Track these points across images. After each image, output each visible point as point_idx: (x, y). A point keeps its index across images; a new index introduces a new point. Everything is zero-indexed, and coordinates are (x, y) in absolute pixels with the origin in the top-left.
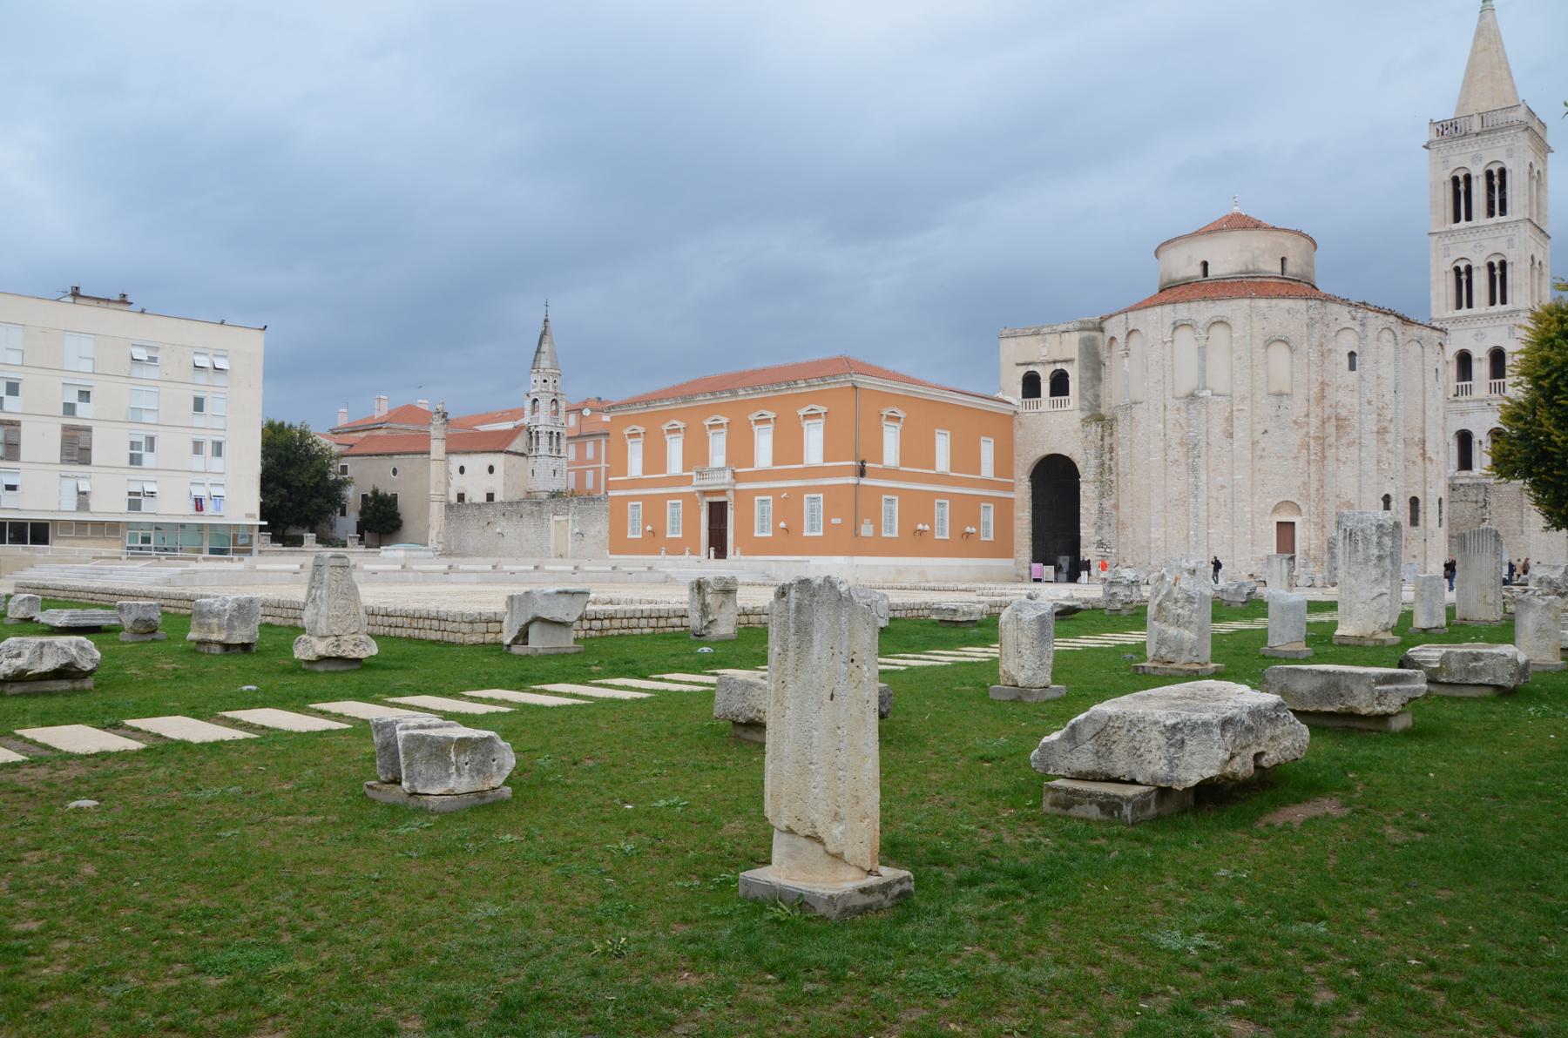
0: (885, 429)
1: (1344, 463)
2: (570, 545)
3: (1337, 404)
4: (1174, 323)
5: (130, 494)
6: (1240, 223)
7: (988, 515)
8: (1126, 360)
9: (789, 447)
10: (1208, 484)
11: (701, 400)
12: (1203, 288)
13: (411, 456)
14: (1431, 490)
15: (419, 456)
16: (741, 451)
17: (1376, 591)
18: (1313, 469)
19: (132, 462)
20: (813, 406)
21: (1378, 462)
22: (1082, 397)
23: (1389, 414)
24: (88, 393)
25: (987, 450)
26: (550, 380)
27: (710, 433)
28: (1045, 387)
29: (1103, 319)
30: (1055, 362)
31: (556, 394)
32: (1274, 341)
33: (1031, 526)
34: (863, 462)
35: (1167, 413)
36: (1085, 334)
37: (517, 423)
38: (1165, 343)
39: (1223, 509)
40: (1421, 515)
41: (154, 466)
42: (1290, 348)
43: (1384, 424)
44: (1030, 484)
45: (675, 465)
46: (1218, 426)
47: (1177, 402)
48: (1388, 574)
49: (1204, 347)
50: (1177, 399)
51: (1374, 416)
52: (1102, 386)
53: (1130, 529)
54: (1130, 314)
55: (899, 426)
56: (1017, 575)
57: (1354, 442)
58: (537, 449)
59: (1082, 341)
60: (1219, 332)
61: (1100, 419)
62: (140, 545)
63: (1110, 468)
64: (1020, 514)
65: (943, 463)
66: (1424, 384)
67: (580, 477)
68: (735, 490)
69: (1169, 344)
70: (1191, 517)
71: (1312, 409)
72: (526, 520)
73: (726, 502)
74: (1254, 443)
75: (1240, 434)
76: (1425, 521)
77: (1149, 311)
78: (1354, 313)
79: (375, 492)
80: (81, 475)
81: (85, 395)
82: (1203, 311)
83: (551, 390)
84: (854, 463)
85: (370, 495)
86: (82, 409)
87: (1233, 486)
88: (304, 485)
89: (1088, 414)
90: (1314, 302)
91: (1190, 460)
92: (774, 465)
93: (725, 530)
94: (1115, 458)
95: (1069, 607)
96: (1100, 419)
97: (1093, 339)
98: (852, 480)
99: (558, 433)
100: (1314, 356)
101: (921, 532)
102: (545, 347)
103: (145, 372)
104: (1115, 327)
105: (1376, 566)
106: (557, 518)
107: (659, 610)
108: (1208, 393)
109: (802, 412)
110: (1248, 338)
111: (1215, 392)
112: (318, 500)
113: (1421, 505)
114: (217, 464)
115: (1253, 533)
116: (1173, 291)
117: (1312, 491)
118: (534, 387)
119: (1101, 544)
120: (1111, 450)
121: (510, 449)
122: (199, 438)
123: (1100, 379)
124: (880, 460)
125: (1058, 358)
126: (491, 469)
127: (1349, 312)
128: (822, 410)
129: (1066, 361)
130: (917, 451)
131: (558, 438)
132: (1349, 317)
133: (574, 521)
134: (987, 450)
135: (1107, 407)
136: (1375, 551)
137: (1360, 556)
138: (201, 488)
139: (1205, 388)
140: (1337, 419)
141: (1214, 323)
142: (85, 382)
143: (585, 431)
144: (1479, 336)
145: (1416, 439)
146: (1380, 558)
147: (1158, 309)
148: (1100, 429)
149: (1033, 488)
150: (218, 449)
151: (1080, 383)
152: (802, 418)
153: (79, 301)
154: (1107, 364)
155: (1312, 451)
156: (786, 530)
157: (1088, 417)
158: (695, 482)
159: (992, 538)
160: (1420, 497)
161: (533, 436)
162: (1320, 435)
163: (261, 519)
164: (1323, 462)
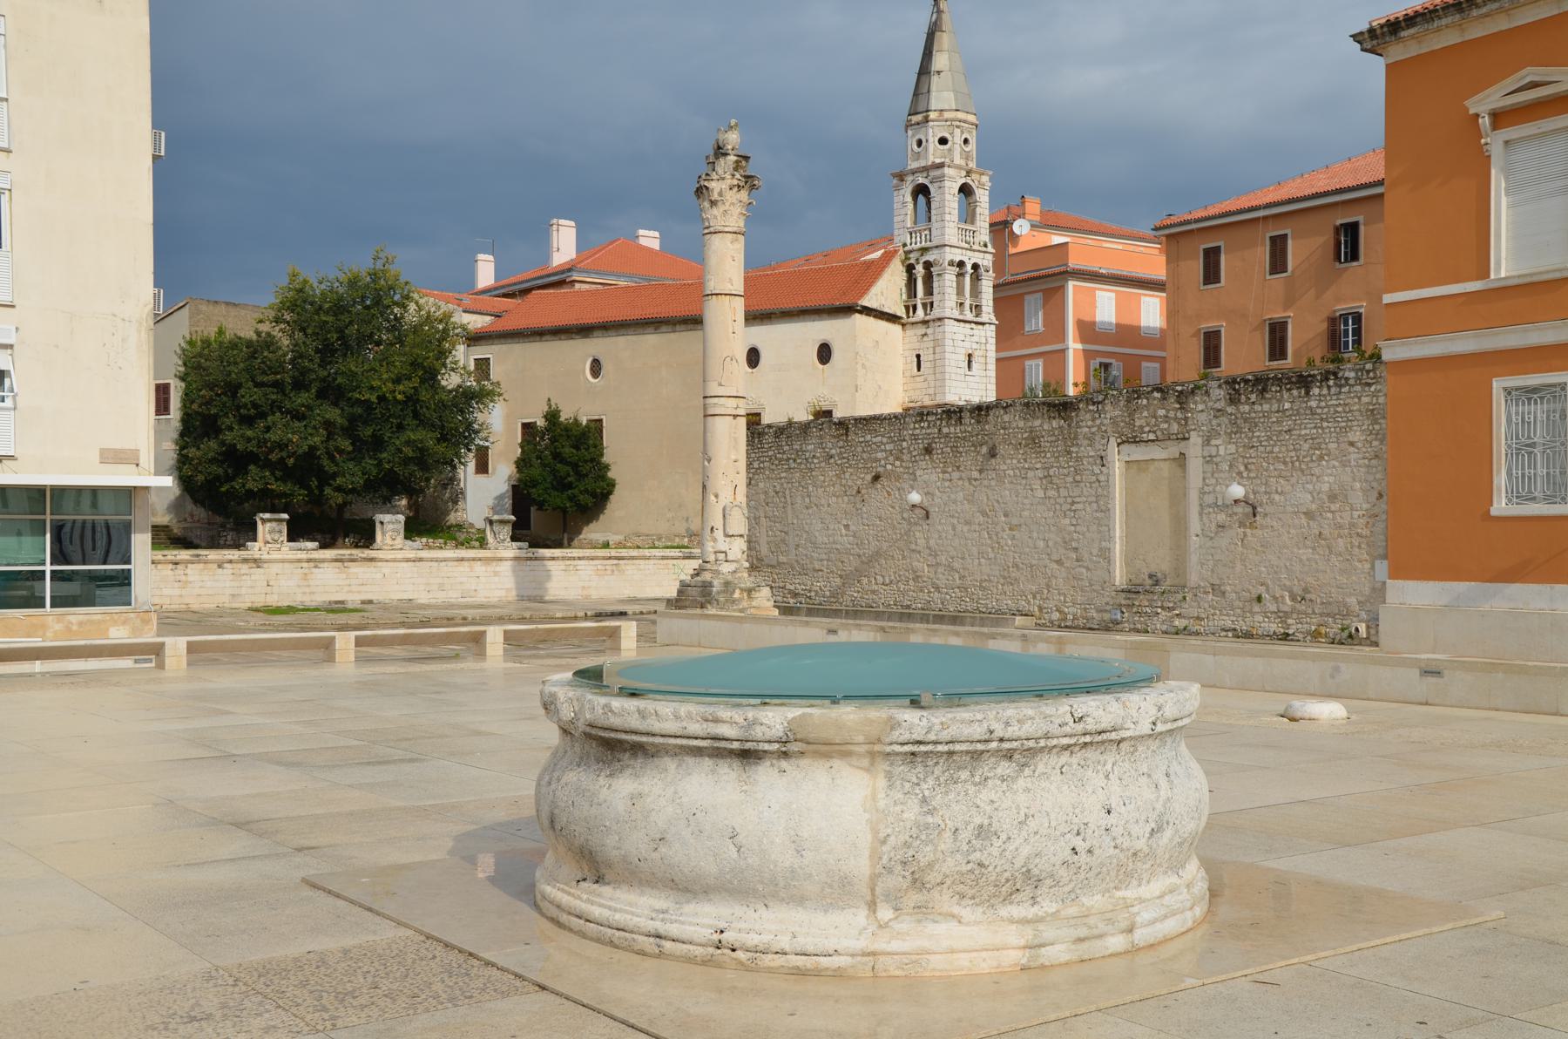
31: (969, 173)
72: (1009, 462)
79: (552, 416)
83: (958, 161)
85: (541, 423)
88: (382, 398)
99: (975, 267)
102: (940, 61)
106: (1138, 453)
118: (917, 156)
121: (866, 302)
133: (1209, 460)
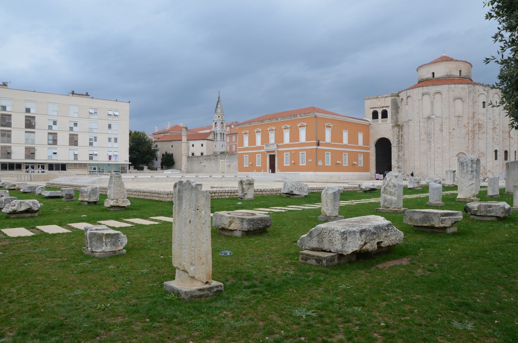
0: (326, 130)
1: (481, 139)
2: (226, 169)
3: (479, 119)
4: (423, 93)
5: (90, 155)
6: (446, 59)
7: (361, 158)
8: (407, 106)
9: (294, 137)
10: (434, 147)
11: (267, 122)
12: (432, 81)
13: (177, 141)
15: (179, 141)
16: (279, 138)
17: (471, 183)
18: (470, 141)
19: (90, 145)
20: (302, 123)
21: (493, 139)
22: (392, 118)
23: (497, 123)
24: (77, 123)
25: (360, 137)
26: (221, 116)
27: (270, 132)
28: (380, 116)
29: (399, 93)
30: (383, 107)
31: (222, 121)
32: (456, 99)
33: (375, 161)
34: (319, 141)
35: (421, 123)
36: (393, 98)
37: (211, 130)
38: (419, 100)
39: (440, 155)
40: (508, 157)
41: (96, 146)
42: (462, 101)
43: (495, 126)
44: (375, 147)
45: (259, 143)
46: (437, 127)
47: (423, 120)
48: (475, 177)
49: (433, 101)
50: (424, 119)
51: (492, 123)
52: (399, 115)
53: (408, 162)
54: (408, 91)
55: (331, 129)
56: (371, 178)
57: (484, 132)
58: (217, 139)
59: (392, 100)
60: (438, 96)
61: (398, 126)
62: (93, 170)
63: (402, 142)
64: (372, 158)
65: (345, 141)
67: (231, 147)
68: (278, 151)
69: (421, 100)
70: (429, 158)
71: (470, 121)
72: (212, 161)
73: (275, 155)
74: (450, 133)
75: (445, 130)
76: (510, 159)
77: (414, 89)
78: (484, 88)
79: (166, 153)
80: (75, 149)
81: (76, 124)
82: (432, 89)
84: (316, 141)
85: (165, 154)
86: (75, 129)
87: (443, 148)
88: (144, 151)
89: (394, 124)
90: (471, 85)
91: (428, 139)
92: (290, 142)
93: (275, 164)
94: (403, 139)
95: (372, 188)
96: (398, 126)
97: (396, 99)
98: (315, 147)
99: (223, 133)
100: (471, 103)
101: (338, 164)
102: (219, 106)
103: (94, 117)
104: (403, 95)
105: (471, 174)
106: (222, 160)
107: (231, 190)
108: (434, 116)
109: (299, 125)
110: (448, 98)
111: (437, 116)
112: (149, 156)
113: (508, 153)
114: (116, 145)
115: (450, 163)
116: (423, 82)
117: (470, 149)
118: (216, 119)
119: (398, 167)
120: (402, 136)
122: (110, 137)
123: (398, 113)
124: (324, 141)
125: (384, 106)
126: (202, 145)
127: (483, 88)
128: (305, 124)
129: (386, 107)
130: (337, 137)
131: (223, 135)
132: (483, 90)
133: (227, 161)
134: (360, 137)
135: (400, 122)
136: (470, 169)
137: (465, 171)
138: (111, 152)
139: (433, 115)
140: (479, 124)
141: (436, 93)
142: (75, 120)
143: (232, 132)
145: (507, 131)
146: (472, 171)
147: (417, 89)
148: (398, 129)
149: (376, 149)
150: (116, 140)
151: (391, 114)
152: (299, 127)
153: (74, 95)
154: (400, 107)
155: (470, 135)
156: (294, 163)
157: (394, 125)
158: (265, 148)
159: (362, 165)
160: (508, 151)
161: (215, 134)
162: (473, 130)
163: (129, 162)
164: (474, 139)
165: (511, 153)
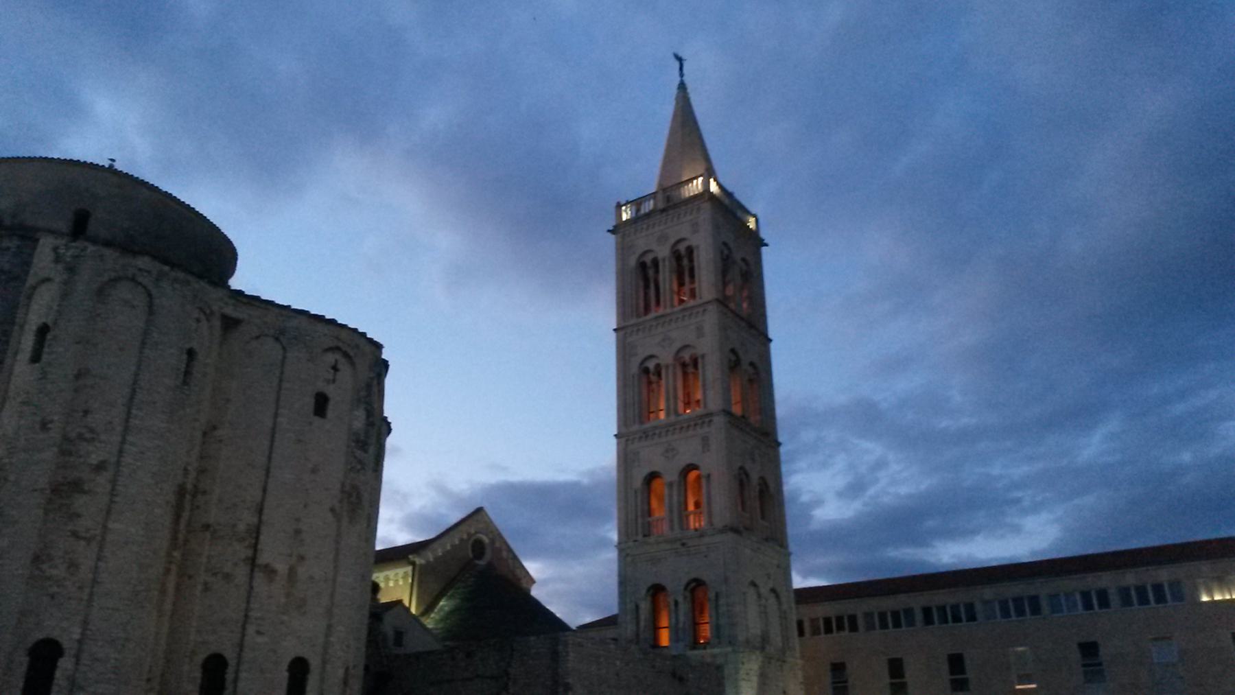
14: (260, 639)
21: (37, 559)
66: (276, 415)
144: (670, 452)
145: (242, 527)
160: (230, 655)
165: (243, 675)
